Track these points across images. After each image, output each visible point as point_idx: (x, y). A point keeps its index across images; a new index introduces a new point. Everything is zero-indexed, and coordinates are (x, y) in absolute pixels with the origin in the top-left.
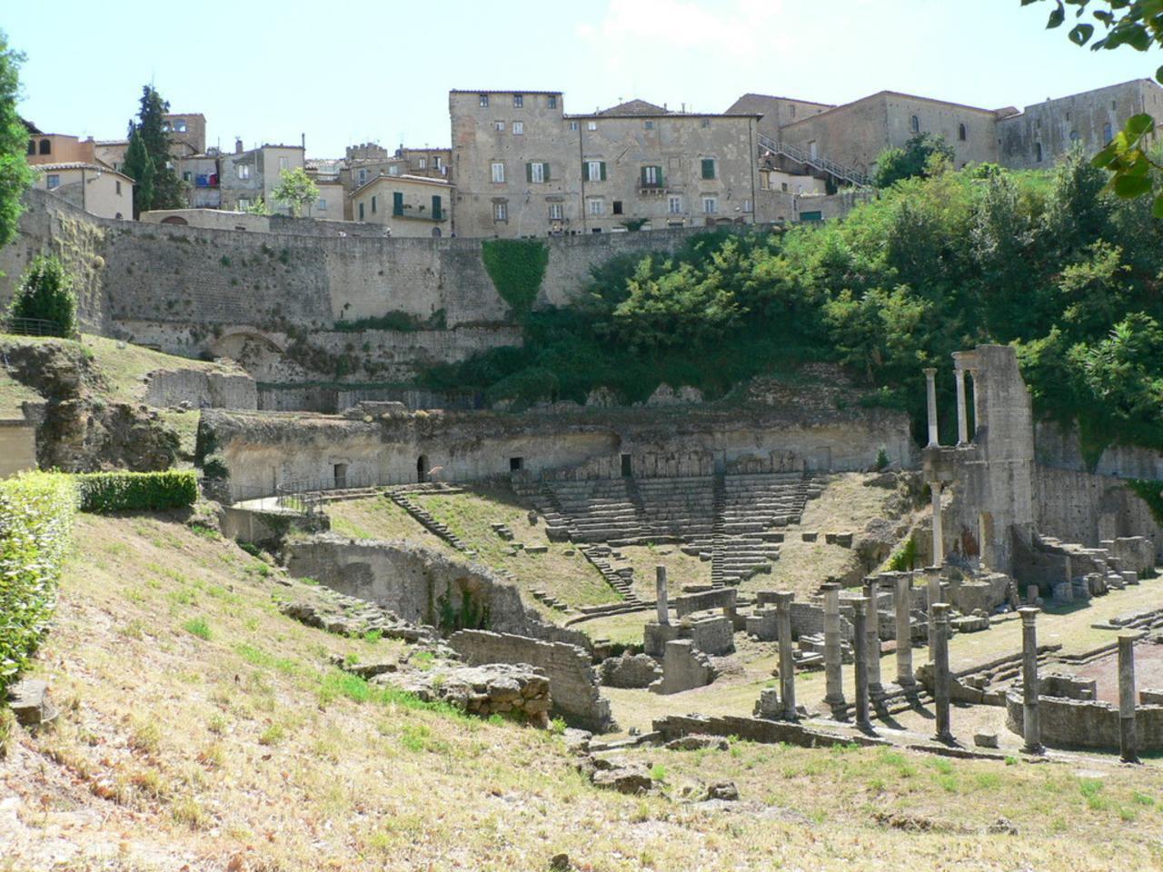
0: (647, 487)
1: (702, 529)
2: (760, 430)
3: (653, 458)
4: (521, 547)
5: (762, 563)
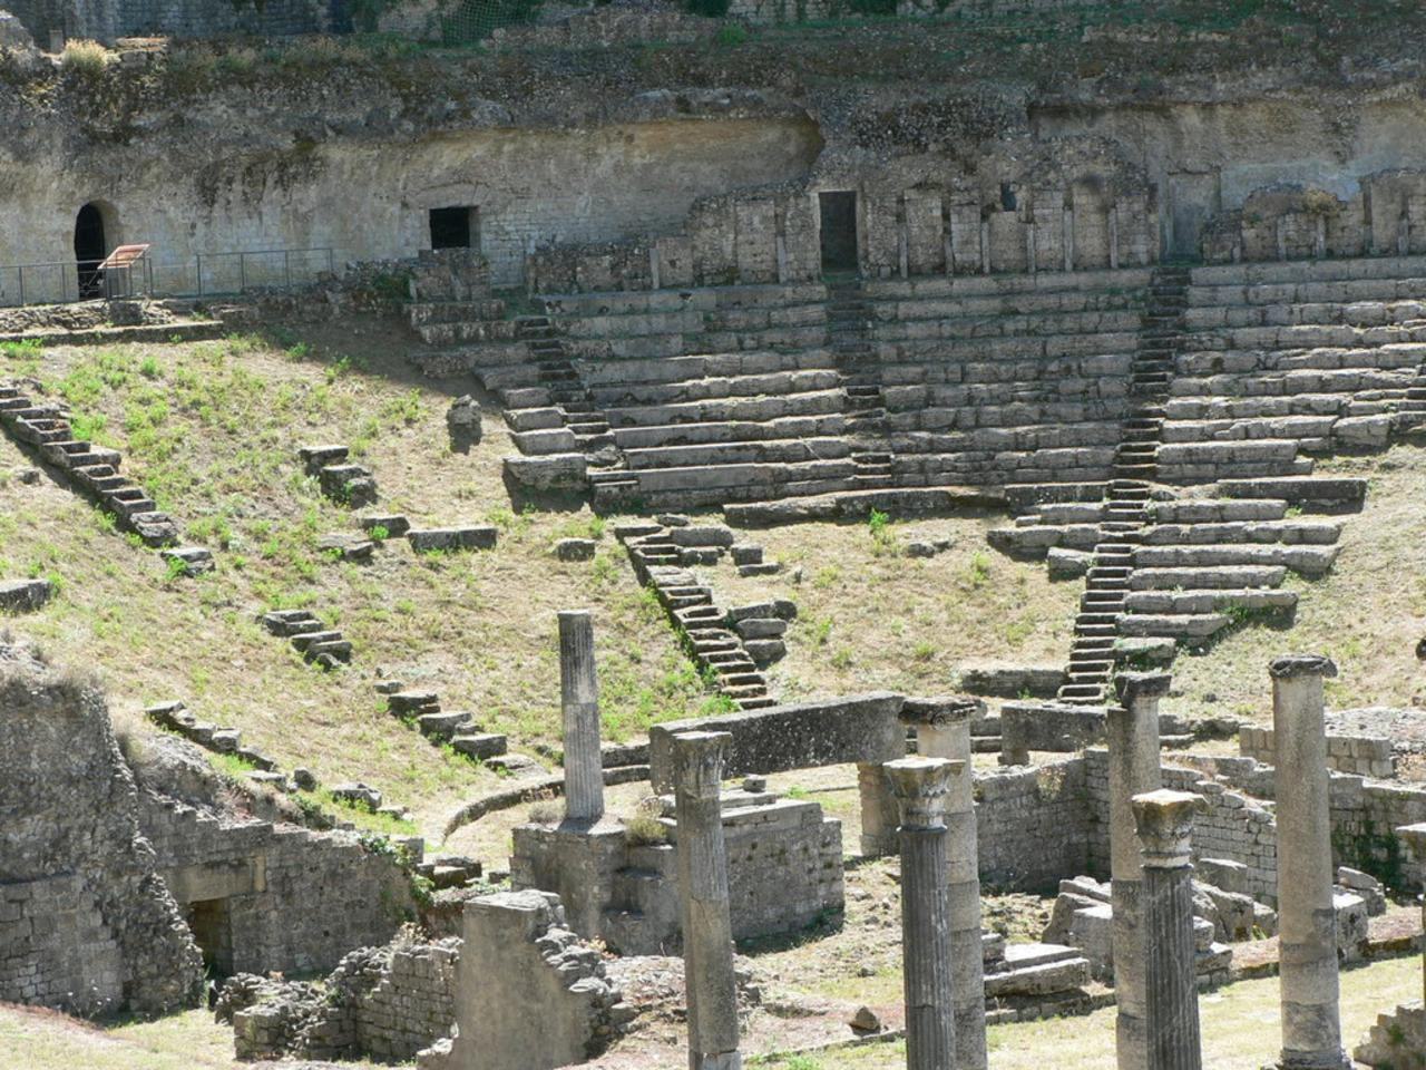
0: (903, 308)
1: (1077, 462)
2: (1341, 98)
3: (934, 204)
4: (398, 527)
5: (1264, 590)
